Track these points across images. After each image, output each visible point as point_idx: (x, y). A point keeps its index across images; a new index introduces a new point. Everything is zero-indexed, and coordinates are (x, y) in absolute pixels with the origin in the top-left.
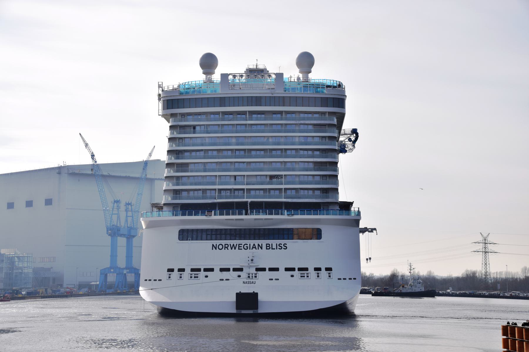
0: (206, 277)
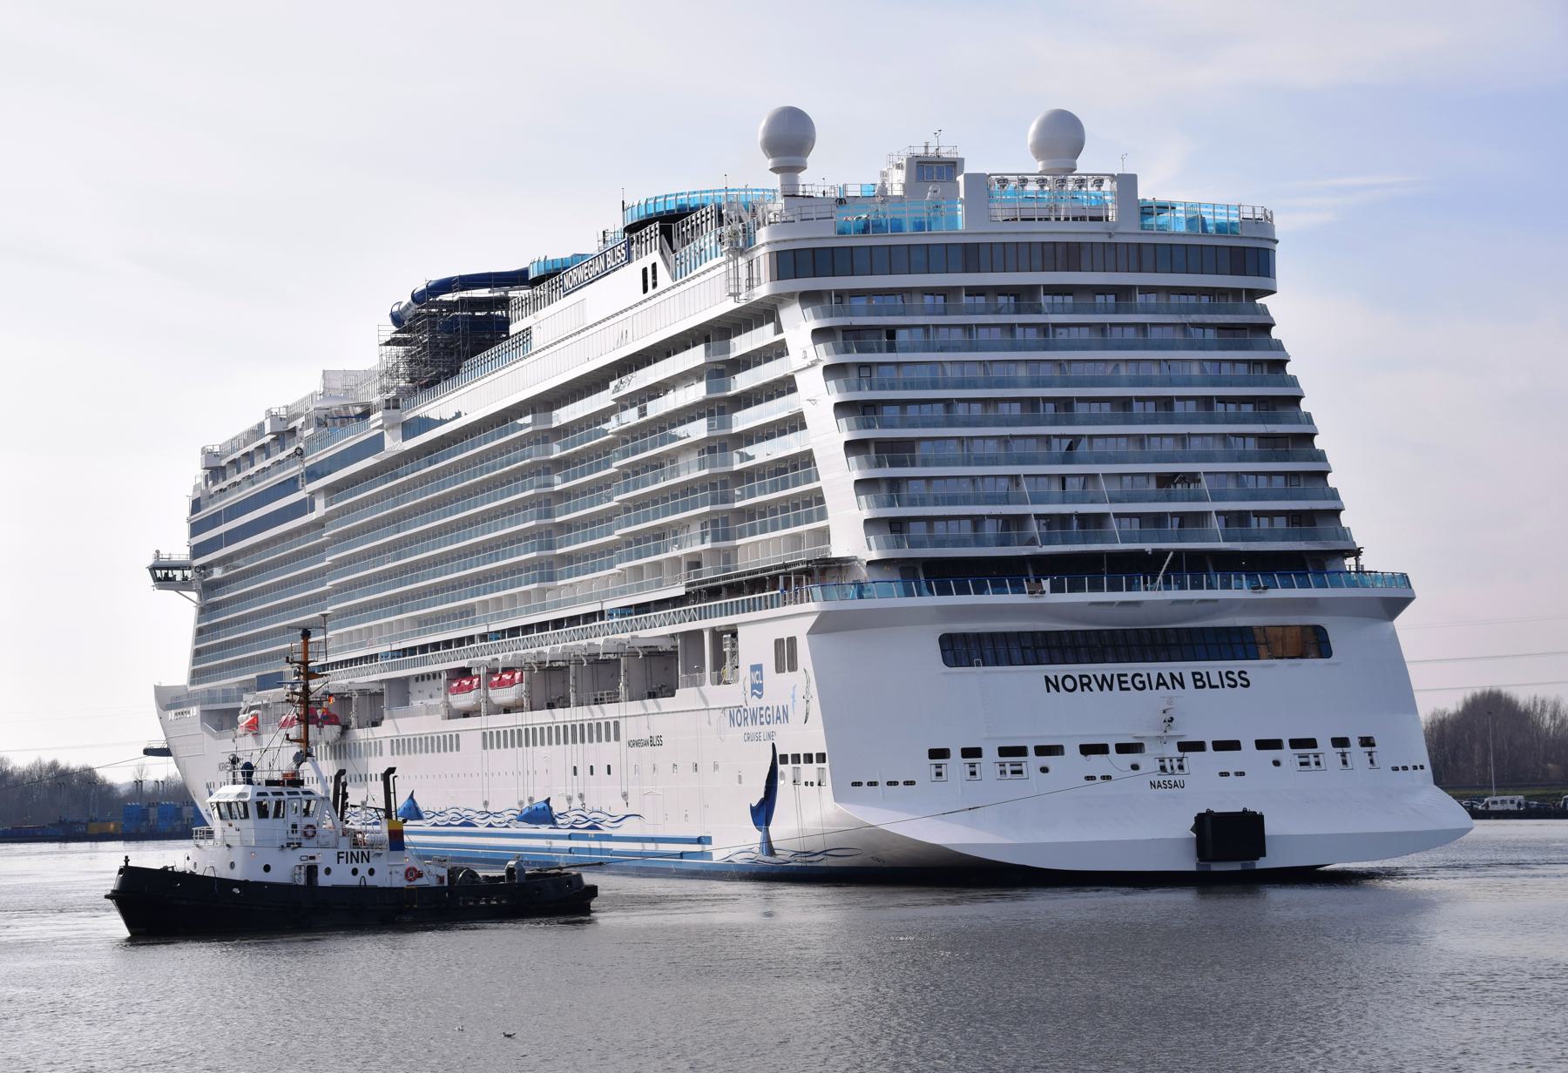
0: (1044, 770)
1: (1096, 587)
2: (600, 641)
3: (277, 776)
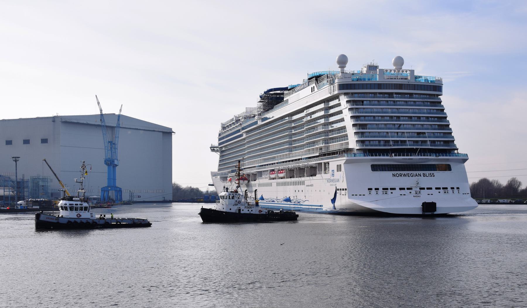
1: (404, 155)
2: (301, 164)
3: (233, 191)
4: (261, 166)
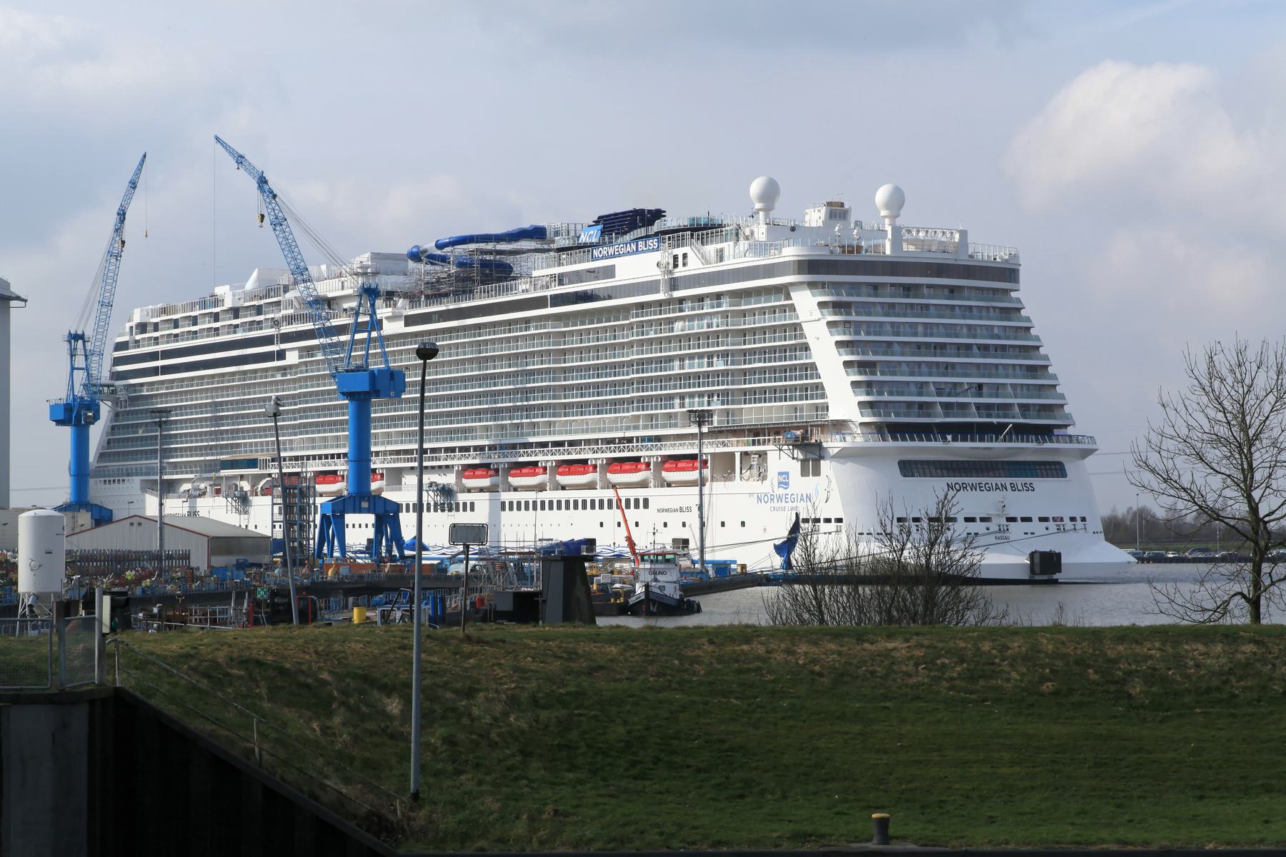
1: (973, 440)
4: (398, 452)
